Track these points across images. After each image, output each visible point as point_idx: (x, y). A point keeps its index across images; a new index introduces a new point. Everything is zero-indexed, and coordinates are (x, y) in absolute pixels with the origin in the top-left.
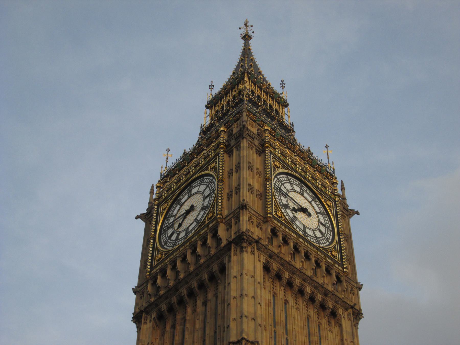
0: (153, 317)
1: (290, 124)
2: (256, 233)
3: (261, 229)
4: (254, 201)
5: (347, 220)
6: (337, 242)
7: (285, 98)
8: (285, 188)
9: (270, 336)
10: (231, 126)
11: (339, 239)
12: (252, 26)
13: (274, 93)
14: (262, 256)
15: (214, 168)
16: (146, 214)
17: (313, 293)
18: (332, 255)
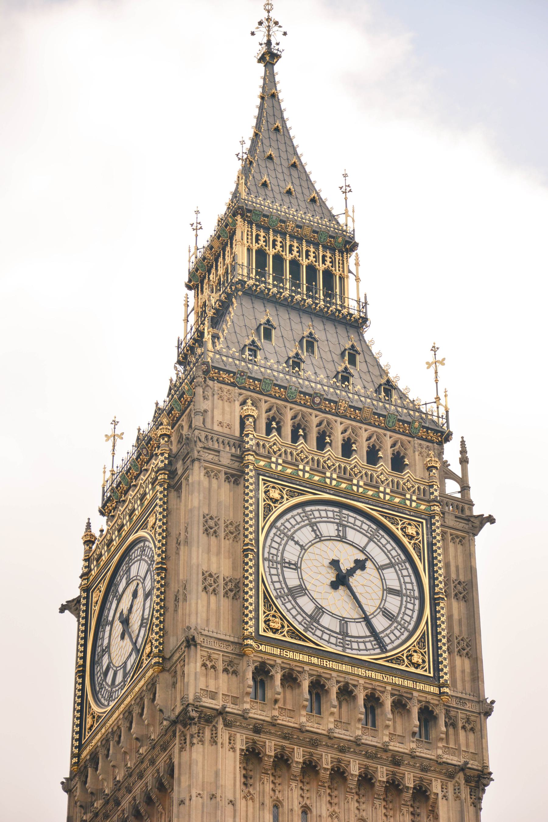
1: (358, 302)
8: (297, 543)
11: (434, 612)
14: (238, 735)
16: (77, 601)
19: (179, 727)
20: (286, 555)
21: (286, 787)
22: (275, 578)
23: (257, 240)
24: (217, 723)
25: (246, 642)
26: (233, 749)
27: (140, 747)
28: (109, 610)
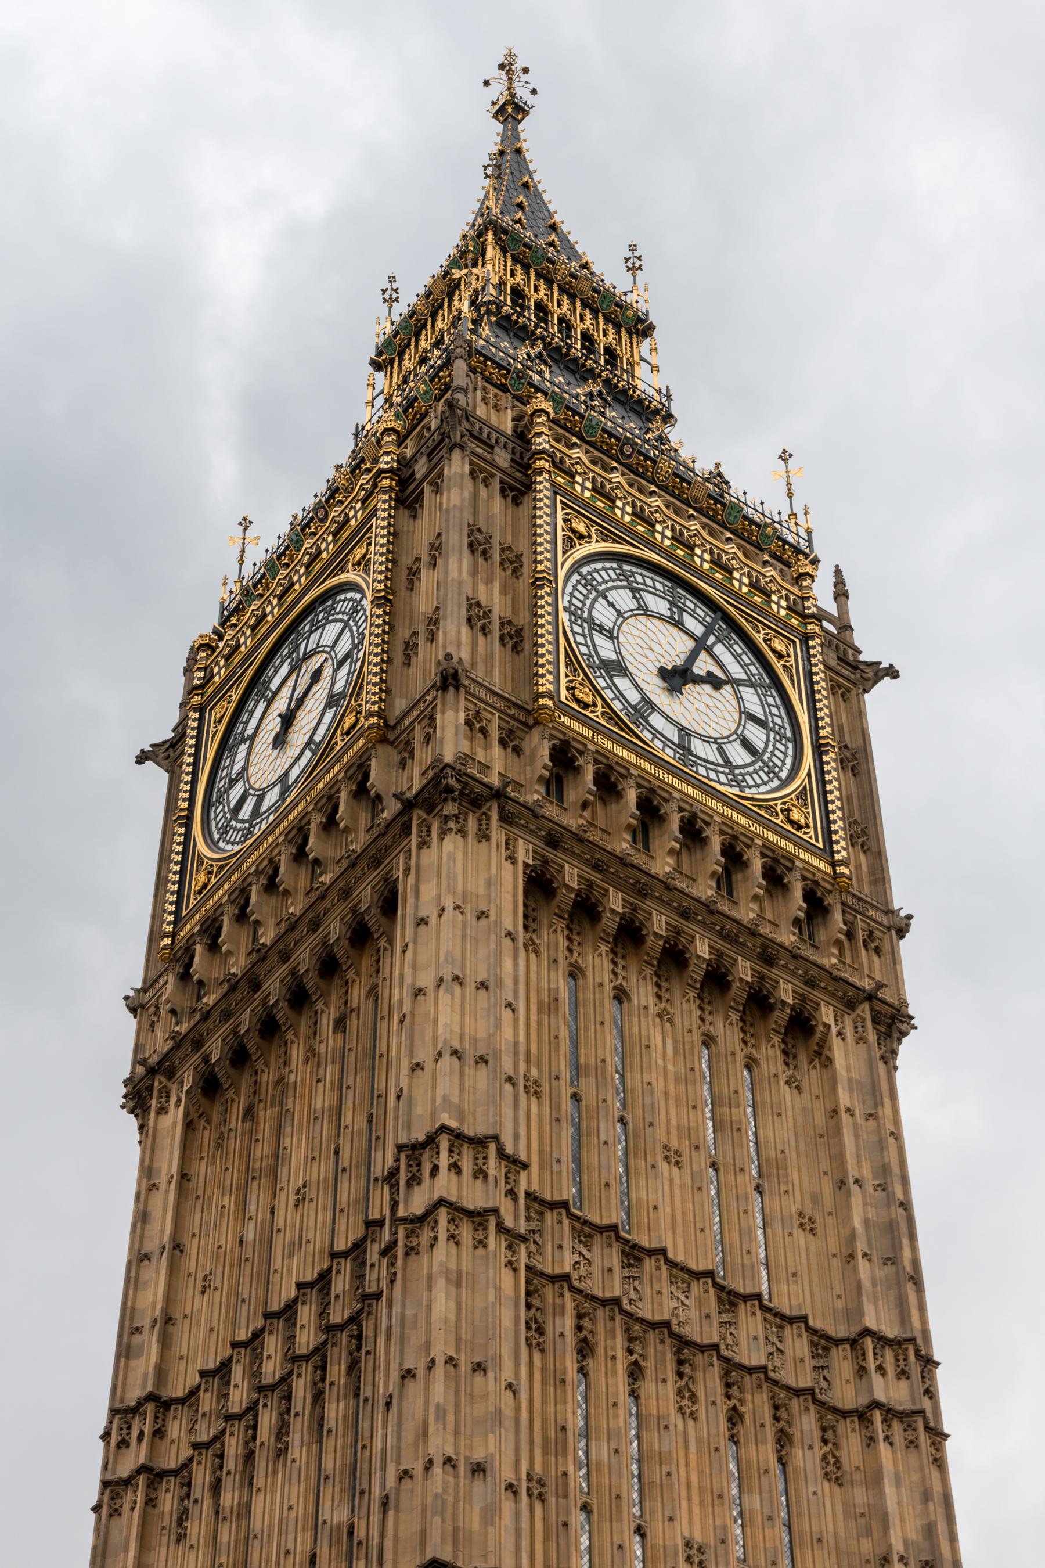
0: (185, 1089)
1: (659, 392)
2: (495, 763)
3: (517, 751)
4: (489, 658)
5: (854, 700)
6: (809, 774)
7: (642, 306)
9: (554, 1115)
10: (427, 413)
11: (819, 764)
12: (526, 71)
13: (598, 292)
14: (521, 842)
15: (363, 562)
17: (719, 955)
18: (792, 822)
19: (417, 815)
20: (595, 613)
21: (590, 951)
22: (580, 639)
23: (513, 275)
24: (489, 809)
25: (541, 701)
26: (512, 859)
27: (321, 875)
28: (247, 723)
